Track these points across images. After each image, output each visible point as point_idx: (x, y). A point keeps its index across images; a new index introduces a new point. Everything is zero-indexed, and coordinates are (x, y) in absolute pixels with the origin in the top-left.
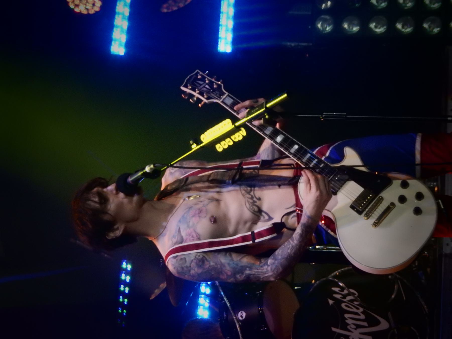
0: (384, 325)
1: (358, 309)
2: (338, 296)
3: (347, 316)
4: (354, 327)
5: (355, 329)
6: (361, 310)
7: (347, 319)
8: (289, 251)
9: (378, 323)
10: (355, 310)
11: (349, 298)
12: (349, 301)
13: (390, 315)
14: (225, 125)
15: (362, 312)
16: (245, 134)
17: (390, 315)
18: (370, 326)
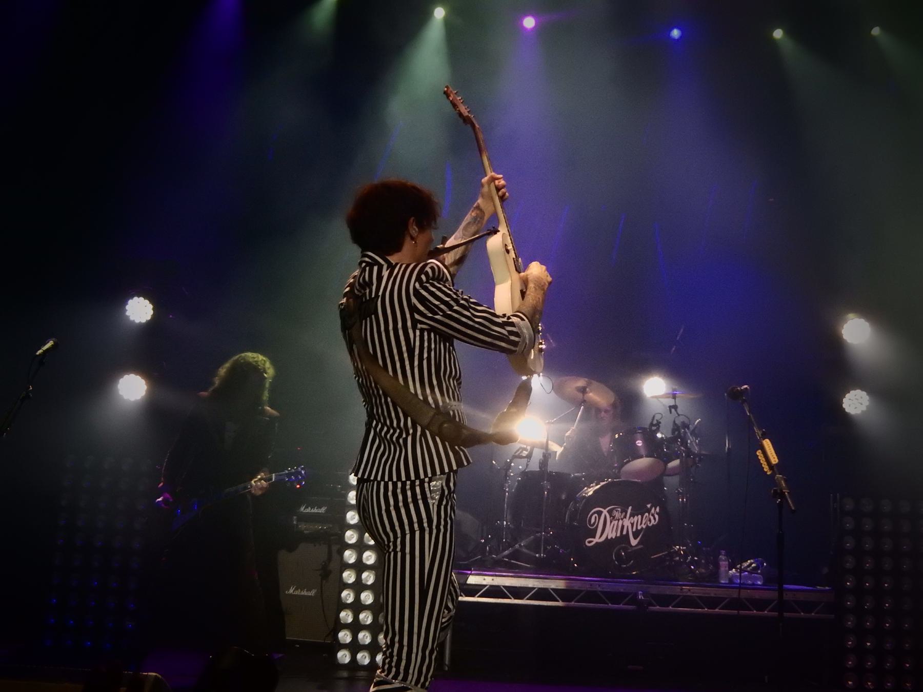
0: (634, 542)
1: (645, 524)
2: (653, 511)
3: (640, 516)
4: (632, 522)
5: (631, 523)
6: (644, 527)
7: (637, 516)
9: (635, 538)
10: (644, 522)
11: (652, 518)
14: (774, 458)
16: (769, 473)
17: (640, 547)
18: (633, 532)
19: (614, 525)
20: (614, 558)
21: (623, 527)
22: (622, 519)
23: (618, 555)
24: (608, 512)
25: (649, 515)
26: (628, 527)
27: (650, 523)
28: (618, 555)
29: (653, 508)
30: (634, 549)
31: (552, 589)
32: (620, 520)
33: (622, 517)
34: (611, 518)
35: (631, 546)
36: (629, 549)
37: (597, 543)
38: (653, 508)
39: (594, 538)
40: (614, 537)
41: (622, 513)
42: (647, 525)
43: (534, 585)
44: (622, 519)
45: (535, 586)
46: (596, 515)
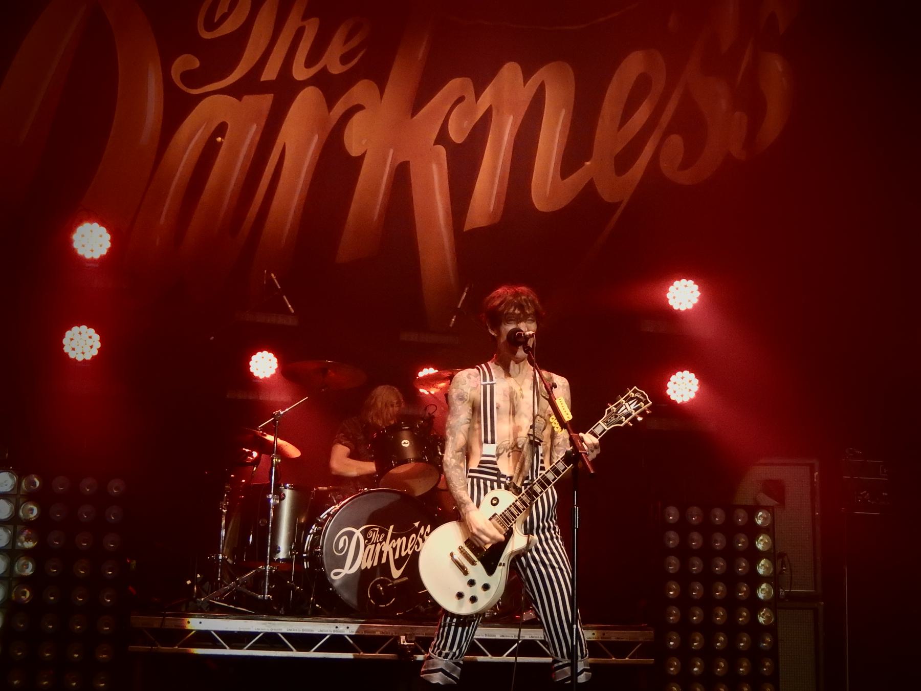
0: (396, 573)
1: (410, 550)
2: (422, 531)
3: (404, 539)
4: (394, 547)
5: (392, 547)
6: (410, 552)
8: (454, 482)
9: (398, 568)
10: (410, 546)
12: (418, 540)
13: (406, 579)
15: (407, 553)
17: (406, 579)
18: (395, 561)
19: (370, 549)
20: (369, 597)
21: (381, 552)
22: (381, 543)
23: (375, 589)
24: (361, 532)
25: (417, 537)
26: (388, 552)
27: (418, 548)
28: (375, 590)
29: (423, 527)
30: (395, 582)
31: (284, 634)
32: (379, 544)
33: (381, 540)
34: (367, 541)
35: (393, 579)
36: (389, 583)
37: (346, 575)
38: (423, 528)
39: (343, 567)
40: (369, 568)
41: (380, 533)
42: (414, 549)
43: (258, 629)
44: (381, 543)
45: (259, 631)
46: (346, 537)
